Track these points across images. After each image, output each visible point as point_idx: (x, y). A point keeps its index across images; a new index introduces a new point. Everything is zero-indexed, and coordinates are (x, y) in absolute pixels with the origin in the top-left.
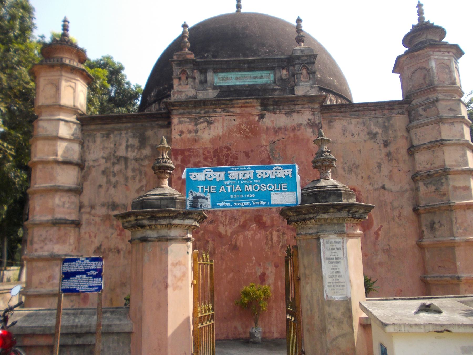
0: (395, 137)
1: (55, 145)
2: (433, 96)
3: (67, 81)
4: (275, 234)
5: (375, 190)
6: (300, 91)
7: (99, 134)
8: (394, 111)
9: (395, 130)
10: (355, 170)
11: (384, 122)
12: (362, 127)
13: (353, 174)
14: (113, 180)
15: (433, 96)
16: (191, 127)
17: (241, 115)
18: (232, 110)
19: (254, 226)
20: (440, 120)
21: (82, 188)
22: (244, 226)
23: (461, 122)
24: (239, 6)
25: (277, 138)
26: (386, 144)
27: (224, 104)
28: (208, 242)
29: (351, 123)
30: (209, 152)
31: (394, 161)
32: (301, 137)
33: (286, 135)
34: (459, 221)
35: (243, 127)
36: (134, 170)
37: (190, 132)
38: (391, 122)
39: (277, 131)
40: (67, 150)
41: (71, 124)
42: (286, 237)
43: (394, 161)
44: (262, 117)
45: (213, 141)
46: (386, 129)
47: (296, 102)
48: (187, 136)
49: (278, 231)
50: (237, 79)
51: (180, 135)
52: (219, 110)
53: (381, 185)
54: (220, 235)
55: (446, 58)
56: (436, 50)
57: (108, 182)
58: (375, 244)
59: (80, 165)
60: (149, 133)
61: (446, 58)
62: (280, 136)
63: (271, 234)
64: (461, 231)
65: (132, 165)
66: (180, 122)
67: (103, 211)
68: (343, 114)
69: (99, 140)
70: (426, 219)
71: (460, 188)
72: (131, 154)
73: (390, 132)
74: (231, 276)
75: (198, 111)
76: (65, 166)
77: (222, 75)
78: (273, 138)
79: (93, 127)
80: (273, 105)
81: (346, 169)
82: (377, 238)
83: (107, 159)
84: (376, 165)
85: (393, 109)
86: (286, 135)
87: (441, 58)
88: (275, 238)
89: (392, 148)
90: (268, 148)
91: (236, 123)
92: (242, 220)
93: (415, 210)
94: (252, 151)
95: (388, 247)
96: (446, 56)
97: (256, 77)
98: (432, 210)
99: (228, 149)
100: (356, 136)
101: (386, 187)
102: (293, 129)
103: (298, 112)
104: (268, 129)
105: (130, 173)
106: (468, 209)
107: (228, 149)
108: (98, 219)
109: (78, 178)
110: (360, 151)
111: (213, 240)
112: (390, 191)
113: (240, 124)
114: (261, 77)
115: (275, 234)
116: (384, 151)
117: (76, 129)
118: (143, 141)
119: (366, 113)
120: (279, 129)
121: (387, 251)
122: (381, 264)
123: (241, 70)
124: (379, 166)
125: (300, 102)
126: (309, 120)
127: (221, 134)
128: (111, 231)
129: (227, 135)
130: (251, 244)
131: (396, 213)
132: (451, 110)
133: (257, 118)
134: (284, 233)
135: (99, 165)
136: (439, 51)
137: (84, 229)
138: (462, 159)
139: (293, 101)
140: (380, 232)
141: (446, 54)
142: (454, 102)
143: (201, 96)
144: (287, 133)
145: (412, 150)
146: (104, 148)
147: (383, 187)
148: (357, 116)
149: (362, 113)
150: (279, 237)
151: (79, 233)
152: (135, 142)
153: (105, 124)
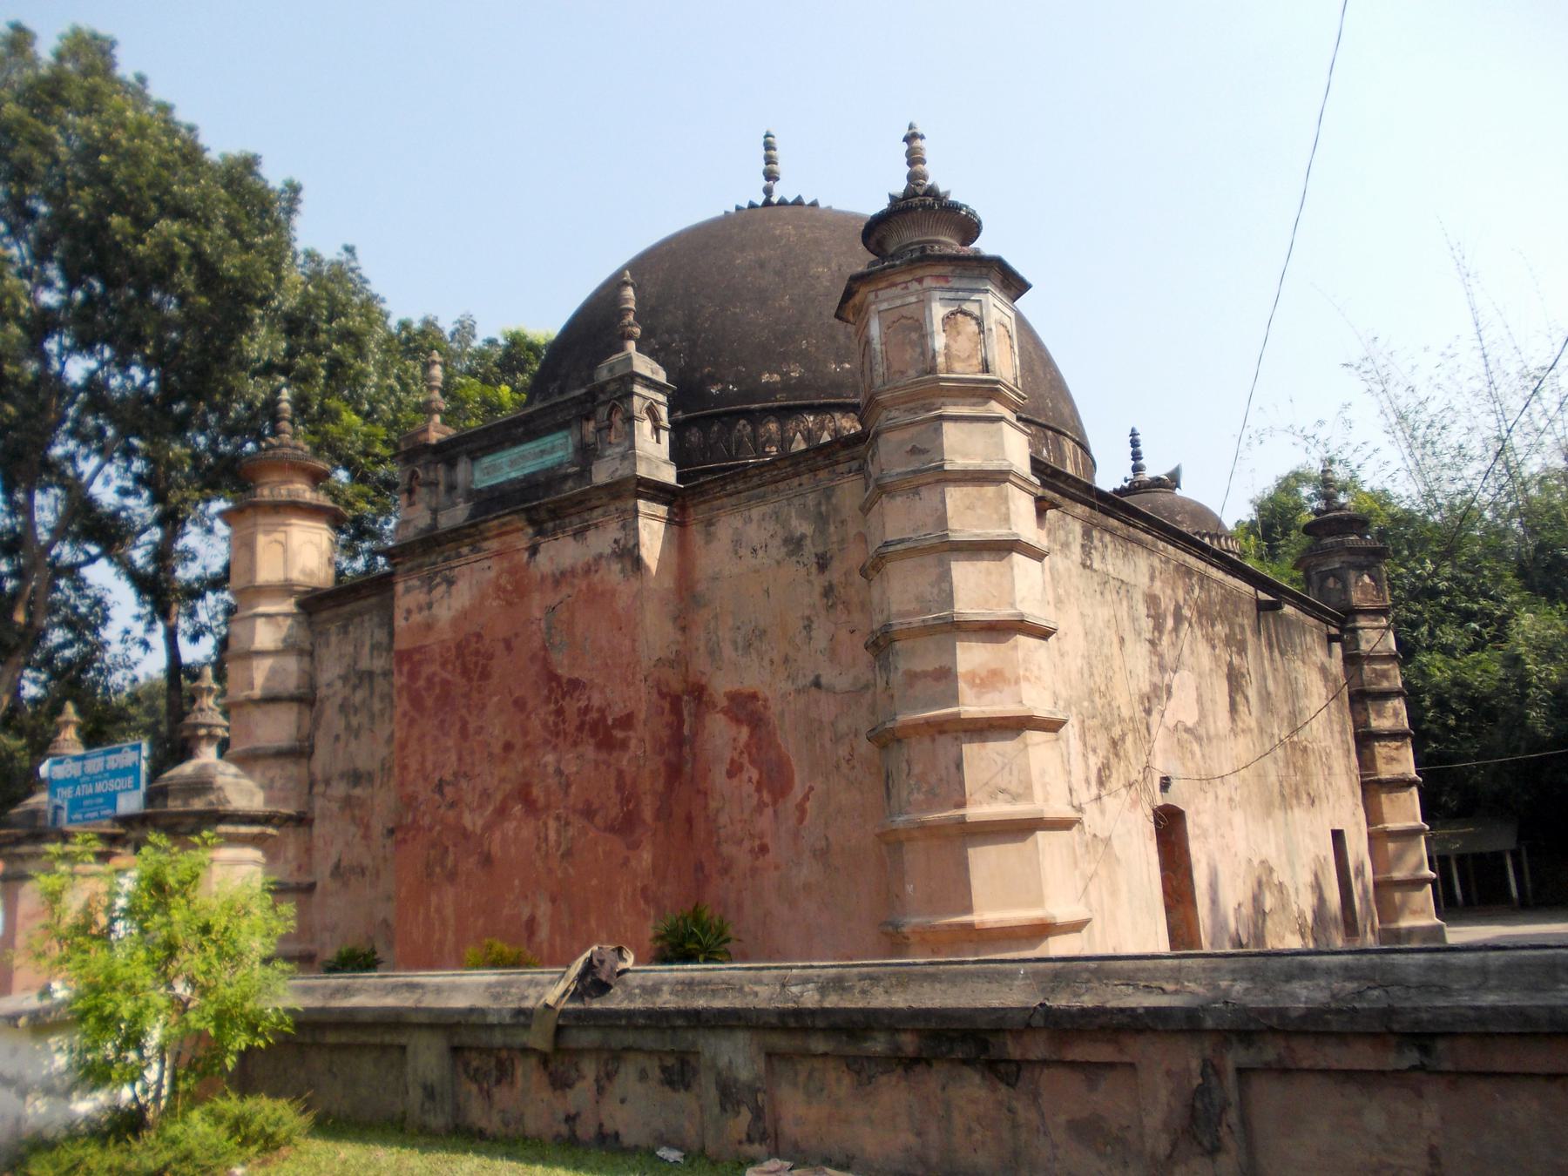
0: (843, 541)
1: (249, 669)
3: (267, 533)
4: (552, 824)
5: (798, 691)
7: (333, 628)
8: (841, 468)
9: (843, 522)
10: (756, 644)
11: (819, 504)
12: (771, 526)
13: (754, 656)
14: (355, 721)
17: (499, 554)
18: (486, 545)
19: (518, 809)
21: (312, 747)
22: (502, 812)
23: (938, 481)
24: (771, 176)
25: (558, 599)
26: (823, 563)
27: (469, 536)
28: (447, 848)
29: (751, 520)
30: (449, 649)
31: (840, 607)
32: (600, 588)
33: (573, 586)
34: (917, 769)
35: (503, 581)
36: (382, 699)
37: (420, 609)
38: (834, 501)
39: (560, 578)
40: (273, 672)
41: (280, 619)
42: (570, 833)
43: (840, 607)
44: (534, 550)
45: (455, 623)
46: (822, 520)
47: (590, 505)
48: (417, 618)
49: (558, 818)
50: (512, 463)
51: (407, 619)
52: (465, 550)
53: (811, 678)
54: (465, 834)
55: (913, 299)
56: (882, 285)
57: (348, 727)
58: (796, 835)
59: (306, 699)
61: (913, 299)
62: (566, 590)
63: (545, 824)
64: (921, 797)
65: (381, 685)
66: (408, 590)
67: (340, 789)
68: (733, 500)
69: (334, 639)
71: (925, 674)
73: (832, 528)
74: (481, 922)
75: (433, 558)
76: (271, 707)
77: (487, 461)
78: (552, 599)
79: (325, 615)
80: (553, 519)
81: (740, 644)
82: (801, 820)
83: (345, 679)
84: (801, 624)
85: (838, 463)
86: (573, 586)
87: (898, 302)
88: (552, 836)
89: (835, 574)
90: (543, 624)
91: (492, 574)
92: (499, 796)
94: (517, 635)
95: (824, 843)
96: (911, 294)
97: (543, 452)
99: (479, 636)
100: (761, 553)
101: (824, 681)
102: (588, 571)
103: (596, 526)
104: (543, 578)
105: (377, 706)
106: (942, 732)
107: (479, 636)
108: (335, 806)
109: (299, 728)
110: (767, 591)
111: (455, 845)
112: (831, 690)
113: (499, 576)
114: (553, 450)
115: (552, 824)
116: (819, 582)
117: (291, 627)
119: (781, 485)
120: (563, 574)
121: (822, 855)
122: (807, 887)
123: (517, 442)
124: (808, 628)
125: (595, 502)
126: (616, 541)
127: (467, 604)
128: (353, 829)
130: (513, 850)
131: (843, 751)
132: (914, 451)
133: (526, 555)
134: (567, 824)
135: (335, 694)
136: (894, 285)
137: (318, 829)
138: (936, 591)
139: (581, 502)
140: (808, 805)
141: (915, 286)
142: (923, 427)
143: (446, 522)
144: (576, 581)
146: (341, 656)
147: (817, 684)
148: (762, 499)
149: (773, 487)
150: (558, 832)
151: (311, 835)
153: (339, 605)
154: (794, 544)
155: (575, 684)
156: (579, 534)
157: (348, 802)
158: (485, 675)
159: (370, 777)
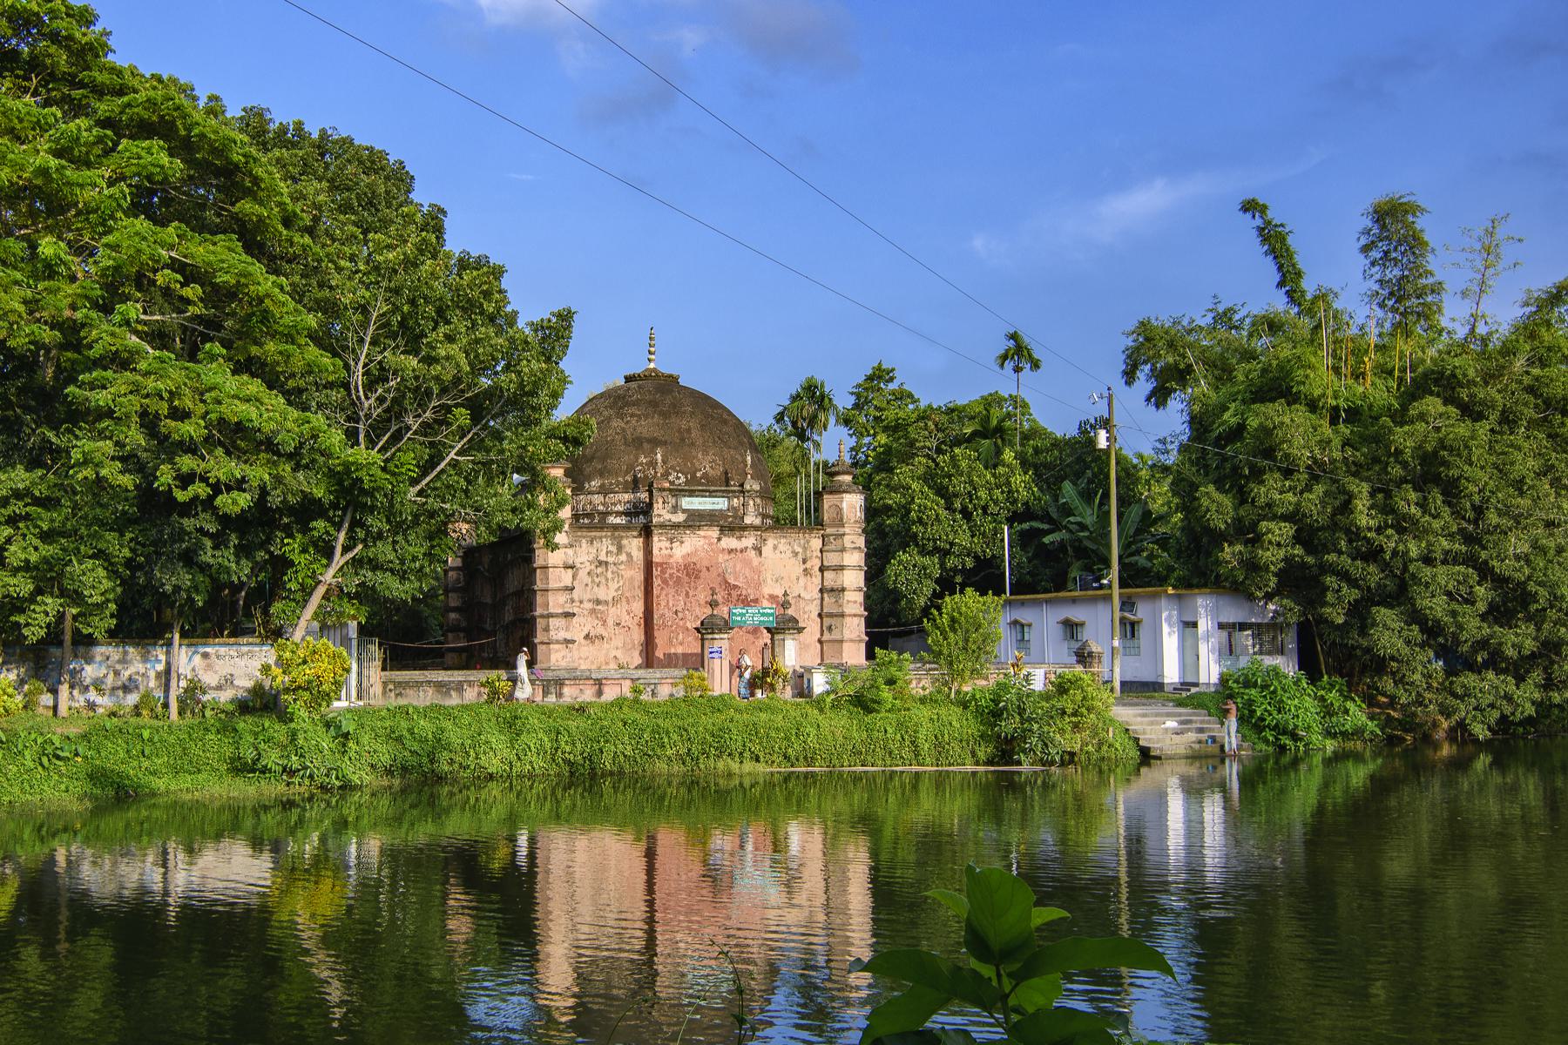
2: (841, 530)
6: (748, 520)
15: (841, 530)
16: (668, 544)
20: (843, 550)
26: (804, 561)
44: (719, 539)
46: (805, 549)
48: (664, 552)
60: (625, 542)
65: (611, 568)
67: (589, 606)
70: (827, 621)
72: (611, 560)
89: (808, 565)
93: (820, 615)
98: (831, 615)
105: (609, 575)
118: (620, 548)
129: (246, 206)
145: (822, 569)
152: (613, 549)
154: (796, 554)
155: (736, 587)
156: (739, 538)
157: (593, 611)
158: (697, 577)
159: (606, 603)
